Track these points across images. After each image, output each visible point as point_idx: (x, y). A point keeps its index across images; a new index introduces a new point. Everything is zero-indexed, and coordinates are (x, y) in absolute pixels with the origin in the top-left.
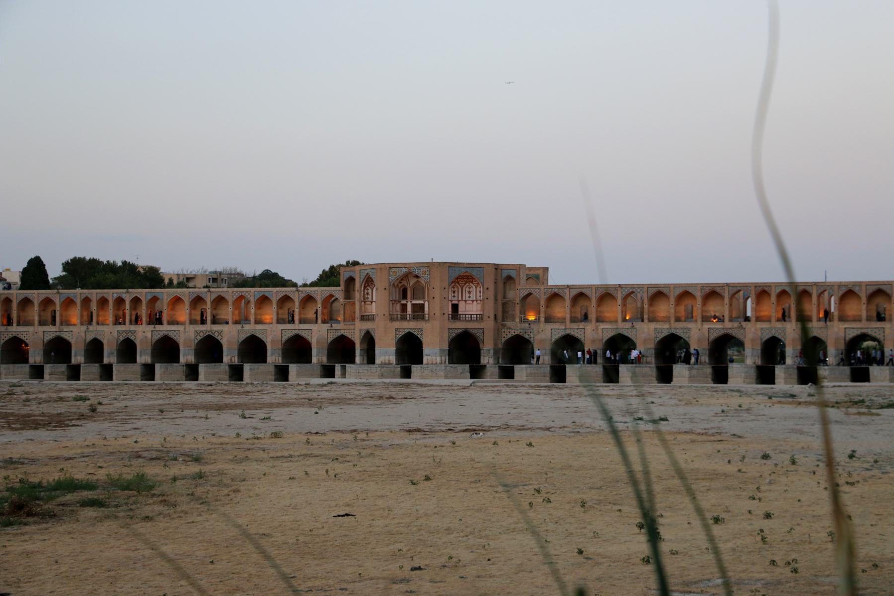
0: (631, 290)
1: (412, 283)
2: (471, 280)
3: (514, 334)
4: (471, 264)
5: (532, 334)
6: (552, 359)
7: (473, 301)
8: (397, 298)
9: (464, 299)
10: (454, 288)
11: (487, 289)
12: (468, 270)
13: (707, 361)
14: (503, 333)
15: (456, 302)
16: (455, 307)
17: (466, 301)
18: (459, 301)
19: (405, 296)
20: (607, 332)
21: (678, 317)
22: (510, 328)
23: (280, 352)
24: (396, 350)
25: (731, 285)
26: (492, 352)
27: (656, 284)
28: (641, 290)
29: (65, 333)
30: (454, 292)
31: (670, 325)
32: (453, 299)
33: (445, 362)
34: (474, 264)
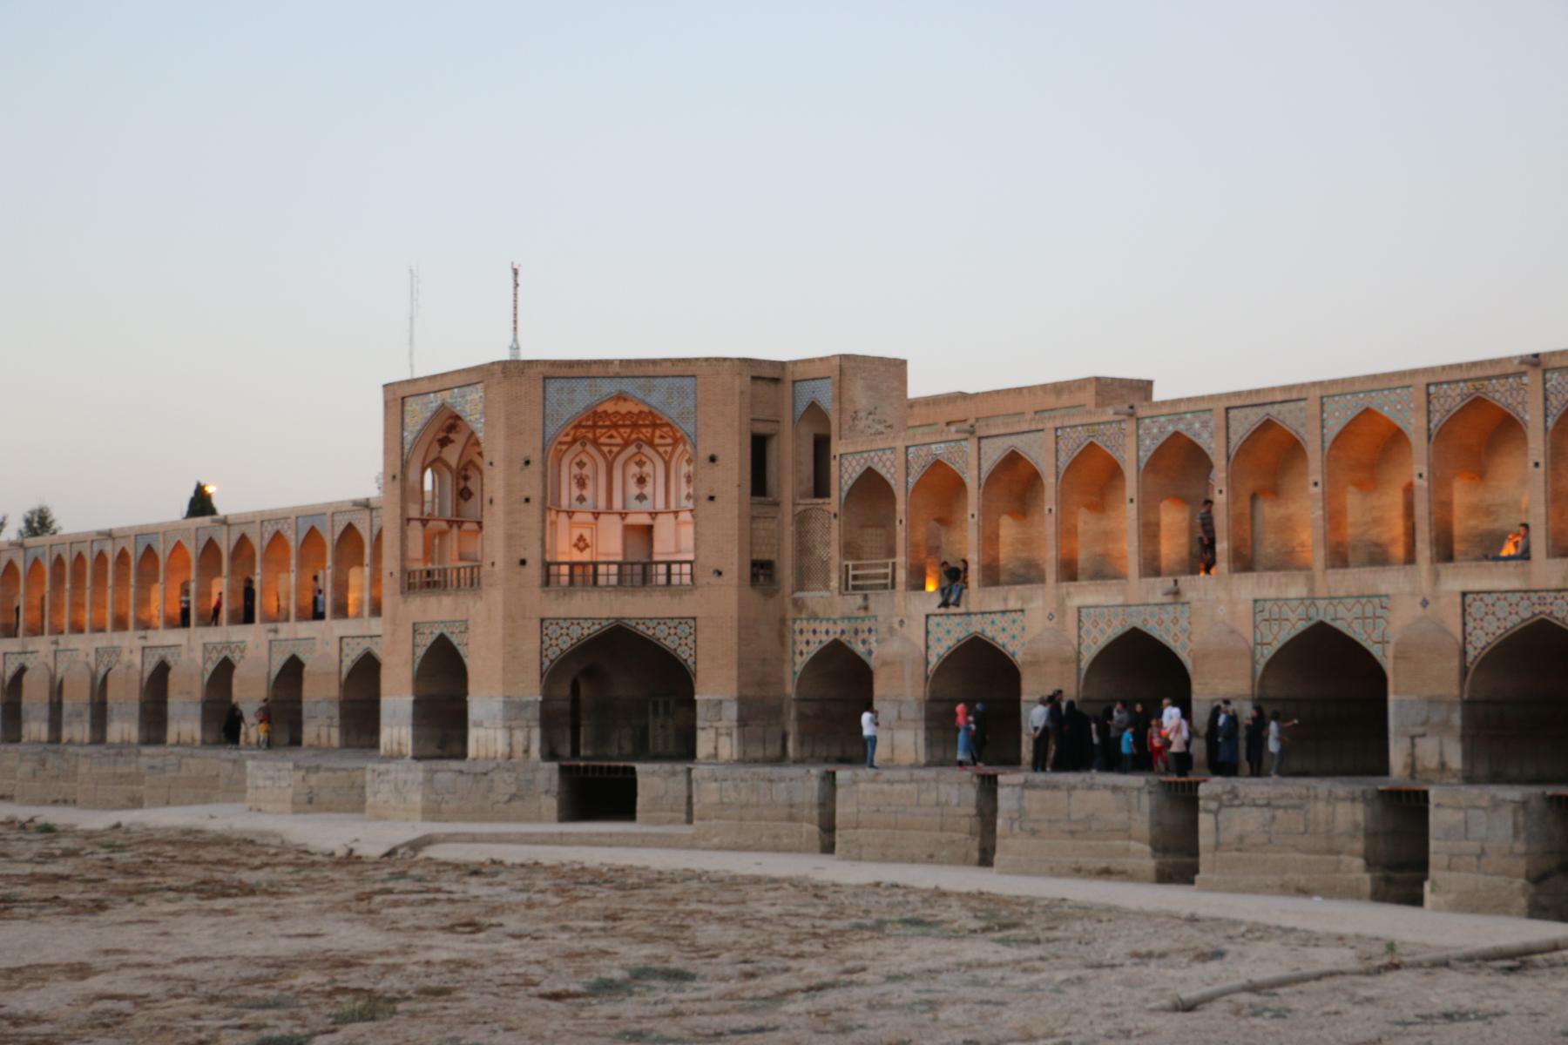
0: (1171, 429)
2: (647, 432)
3: (826, 639)
4: (639, 362)
5: (872, 639)
6: (930, 743)
9: (673, 507)
10: (640, 464)
11: (713, 459)
12: (627, 386)
13: (1455, 760)
14: (798, 638)
15: (645, 520)
17: (676, 513)
18: (654, 515)
20: (1096, 624)
21: (1378, 545)
22: (814, 617)
23: (335, 711)
24: (415, 702)
25: (1556, 362)
26: (731, 712)
27: (1258, 392)
28: (1205, 425)
29: (32, 657)
30: (641, 481)
31: (1310, 581)
32: (634, 505)
33: (527, 751)
34: (654, 362)
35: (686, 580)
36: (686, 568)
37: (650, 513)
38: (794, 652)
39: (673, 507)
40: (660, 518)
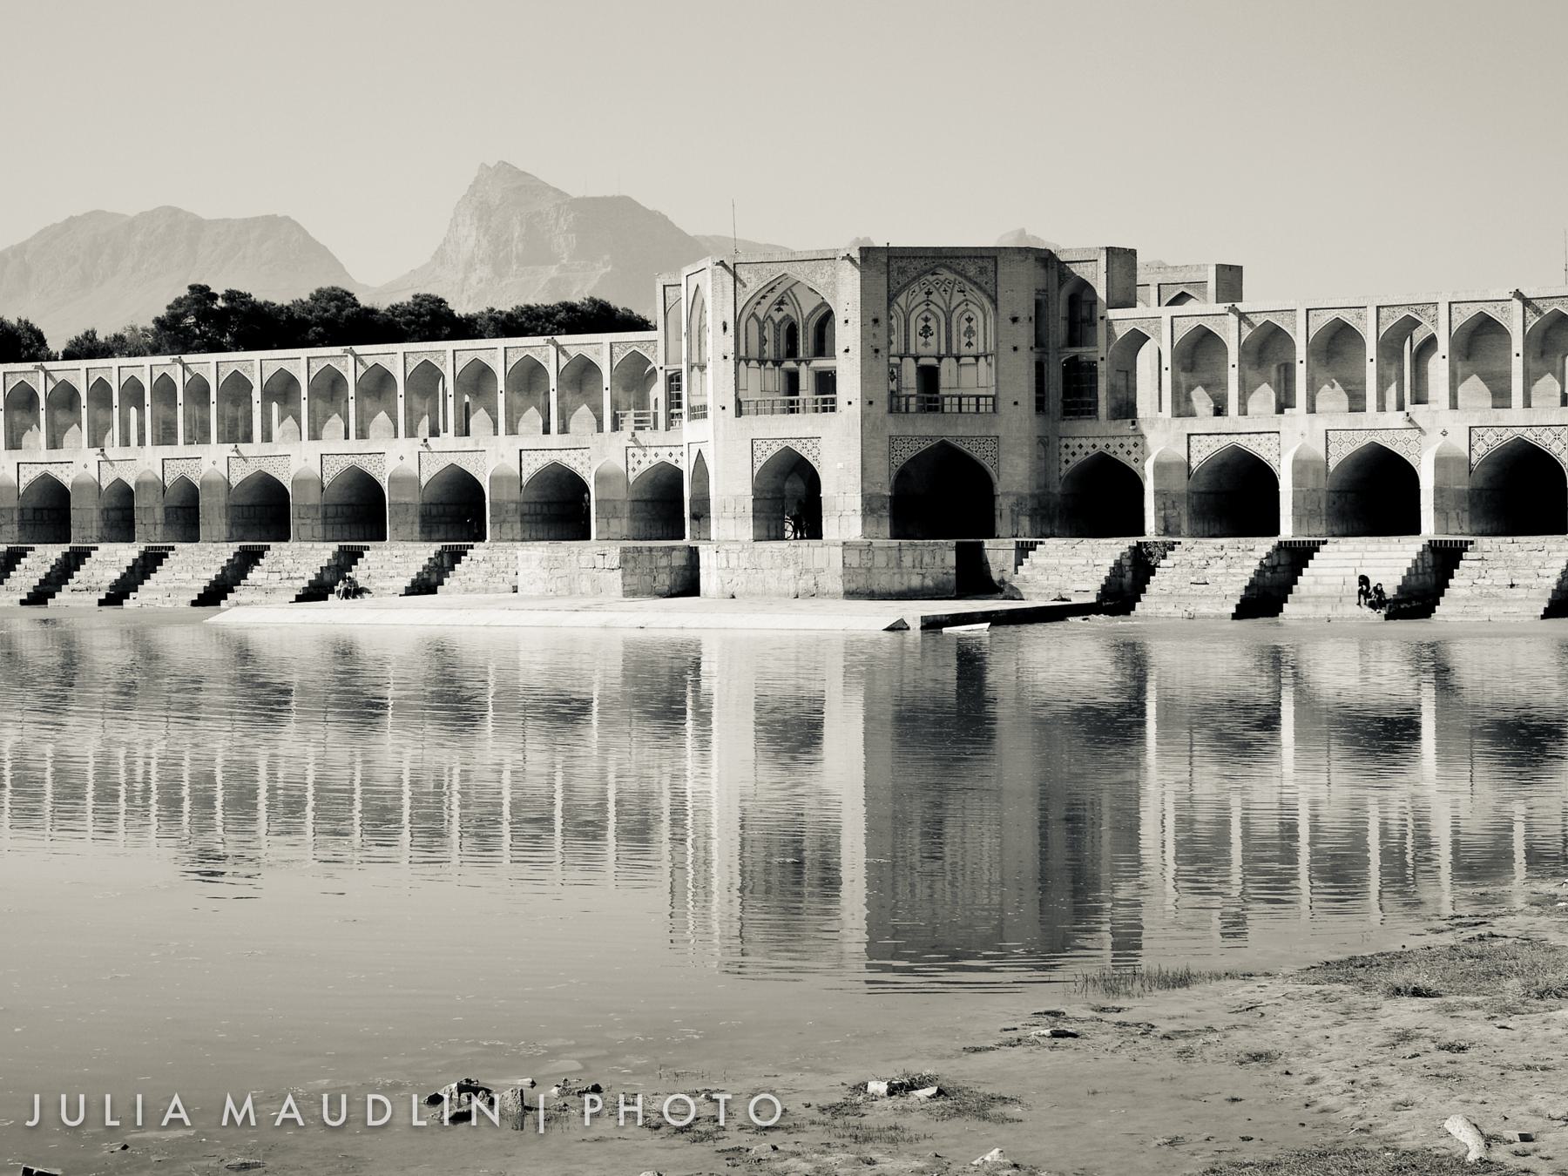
1: (806, 312)
3: (1092, 452)
7: (977, 358)
8: (769, 350)
9: (955, 351)
10: (926, 320)
14: (1063, 450)
15: (934, 362)
16: (929, 377)
17: (958, 358)
18: (940, 359)
19: (792, 353)
32: (922, 350)
35: (990, 409)
36: (990, 400)
37: (937, 358)
38: (1060, 462)
39: (955, 351)
40: (945, 361)
